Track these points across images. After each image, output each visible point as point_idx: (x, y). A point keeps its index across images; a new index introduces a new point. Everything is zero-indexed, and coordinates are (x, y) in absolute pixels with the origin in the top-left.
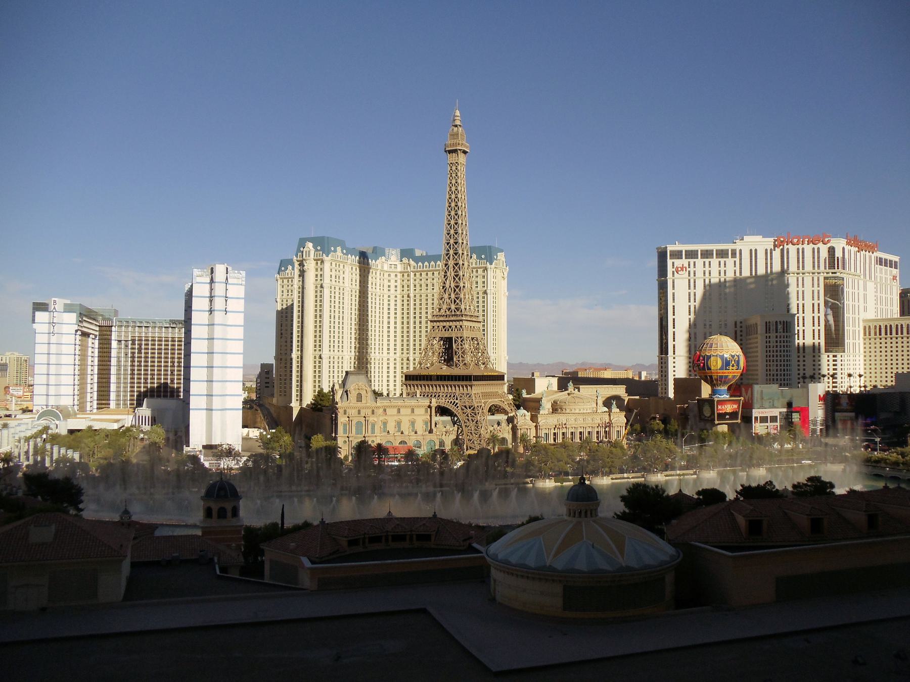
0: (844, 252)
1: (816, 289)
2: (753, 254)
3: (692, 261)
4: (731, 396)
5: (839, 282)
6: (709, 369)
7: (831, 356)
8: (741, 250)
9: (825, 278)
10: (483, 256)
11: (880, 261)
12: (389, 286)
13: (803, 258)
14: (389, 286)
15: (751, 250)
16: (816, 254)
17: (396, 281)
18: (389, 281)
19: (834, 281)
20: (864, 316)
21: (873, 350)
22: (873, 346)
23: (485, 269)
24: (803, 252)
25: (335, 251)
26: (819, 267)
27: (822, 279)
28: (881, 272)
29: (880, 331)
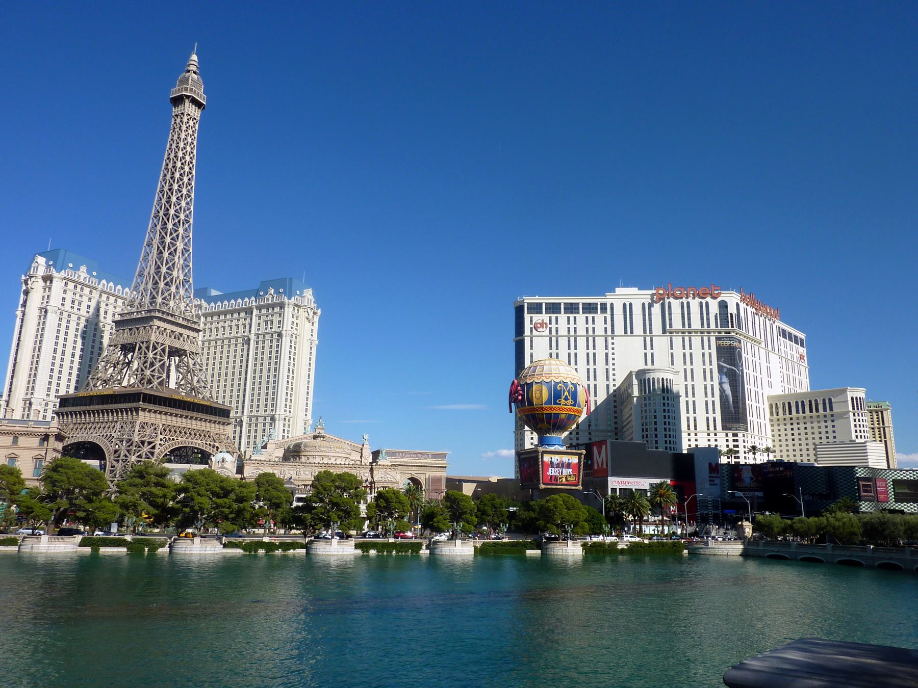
0: (738, 309)
1: (706, 351)
2: (628, 309)
3: (554, 316)
4: (568, 448)
5: (736, 344)
6: (531, 403)
7: (730, 435)
8: (612, 304)
9: (717, 339)
11: (784, 333)
13: (689, 314)
15: (625, 305)
16: (704, 310)
19: (728, 343)
20: (768, 392)
21: (783, 438)
22: (783, 433)
23: (282, 306)
24: (688, 307)
25: (76, 268)
26: (708, 325)
27: (713, 339)
28: (786, 346)
29: (789, 409)
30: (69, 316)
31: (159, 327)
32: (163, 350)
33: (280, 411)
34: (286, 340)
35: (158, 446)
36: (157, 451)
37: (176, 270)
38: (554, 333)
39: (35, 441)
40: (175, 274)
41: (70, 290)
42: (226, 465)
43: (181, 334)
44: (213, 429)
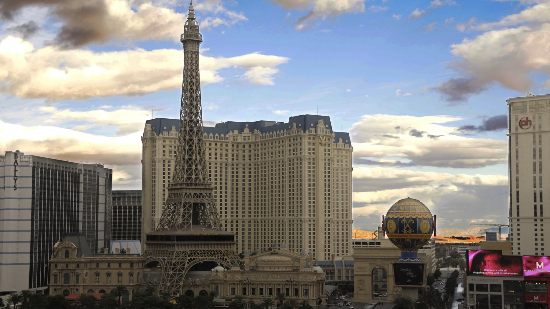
10: (300, 125)
12: (244, 156)
14: (244, 156)
17: (250, 151)
18: (244, 151)
25: (170, 129)
30: (169, 162)
31: (186, 194)
32: (190, 206)
33: (306, 216)
34: (305, 164)
35: (186, 264)
36: (186, 266)
37: (195, 155)
38: (537, 129)
39: (128, 265)
40: (194, 158)
41: (167, 145)
42: (218, 274)
43: (201, 194)
44: (223, 249)
